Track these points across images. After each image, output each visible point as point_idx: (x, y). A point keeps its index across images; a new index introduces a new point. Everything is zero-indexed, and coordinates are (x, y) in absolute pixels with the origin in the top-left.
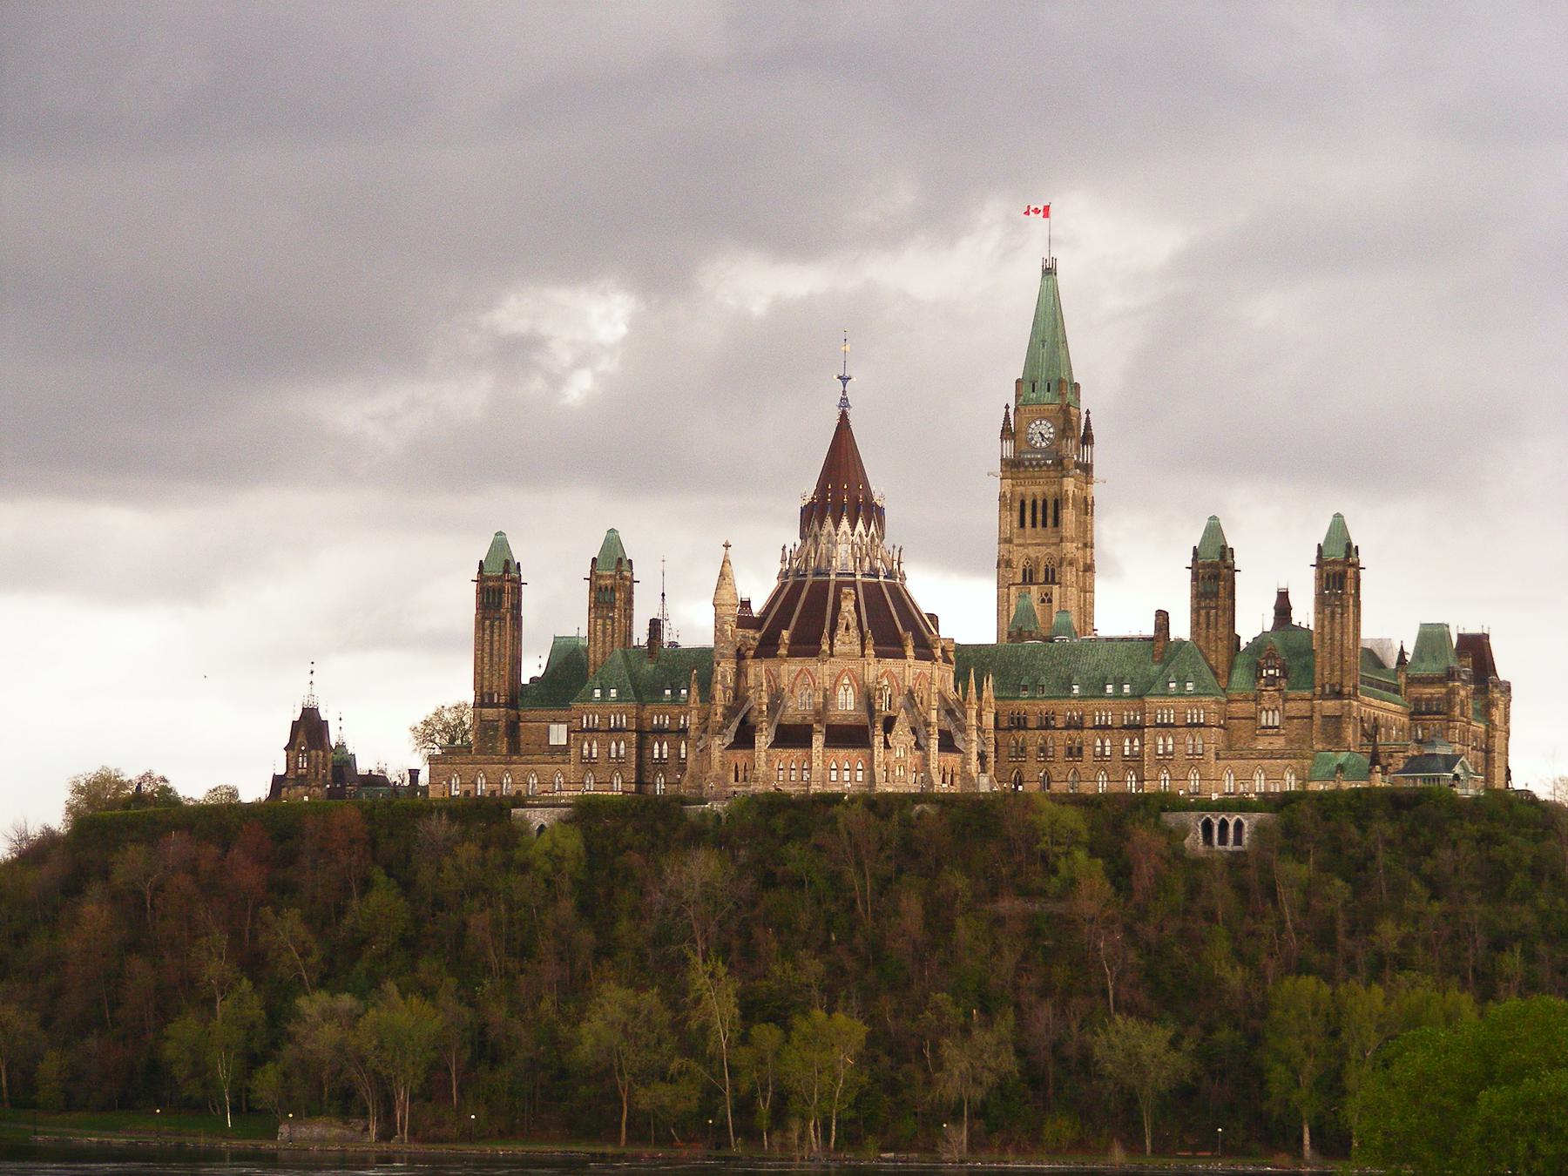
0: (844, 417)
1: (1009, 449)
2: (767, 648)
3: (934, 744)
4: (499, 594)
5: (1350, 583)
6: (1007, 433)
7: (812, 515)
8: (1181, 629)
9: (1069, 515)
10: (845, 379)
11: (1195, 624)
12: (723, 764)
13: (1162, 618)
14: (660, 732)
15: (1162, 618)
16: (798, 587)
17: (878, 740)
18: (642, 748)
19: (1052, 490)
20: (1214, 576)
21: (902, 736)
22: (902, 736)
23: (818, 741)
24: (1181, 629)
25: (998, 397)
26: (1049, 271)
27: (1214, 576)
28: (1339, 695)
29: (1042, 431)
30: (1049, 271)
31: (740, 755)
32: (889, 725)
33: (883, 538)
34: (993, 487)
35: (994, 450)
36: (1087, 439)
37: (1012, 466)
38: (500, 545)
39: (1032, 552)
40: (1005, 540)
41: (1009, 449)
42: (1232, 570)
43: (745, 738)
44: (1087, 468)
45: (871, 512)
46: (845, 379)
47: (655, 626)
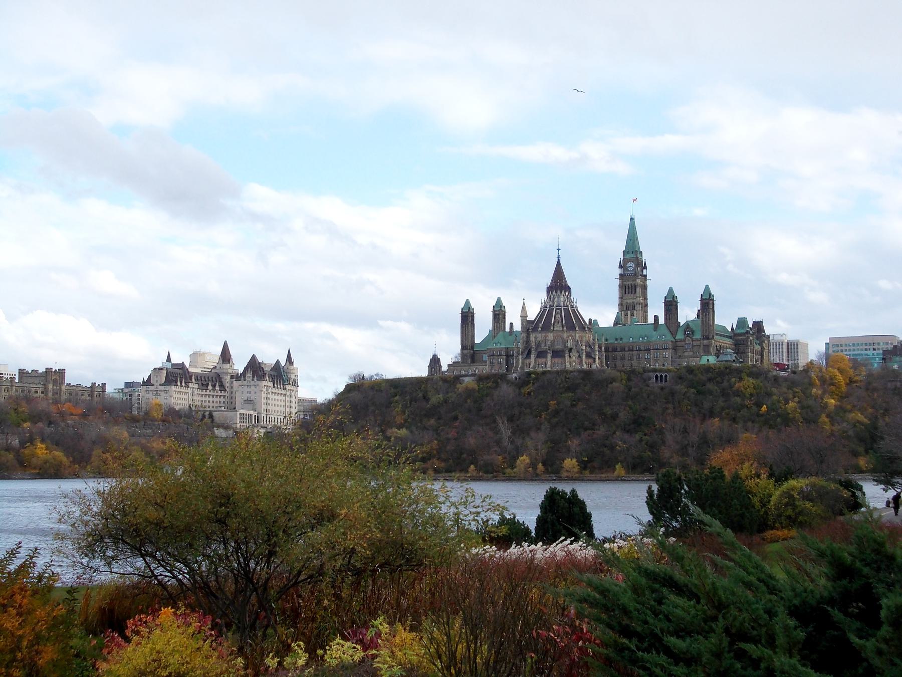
1: (621, 271)
2: (535, 329)
3: (584, 356)
4: (467, 317)
5: (711, 307)
6: (620, 267)
7: (550, 289)
8: (662, 321)
9: (639, 290)
11: (666, 319)
12: (523, 363)
16: (545, 310)
17: (567, 355)
18: (507, 360)
20: (671, 305)
21: (574, 355)
22: (574, 355)
23: (549, 356)
25: (618, 255)
26: (632, 219)
27: (671, 305)
28: (708, 339)
29: (631, 266)
30: (632, 219)
31: (527, 361)
32: (570, 350)
34: (618, 282)
35: (618, 272)
36: (645, 267)
37: (622, 276)
38: (467, 302)
39: (628, 301)
40: (621, 298)
41: (621, 271)
42: (677, 302)
43: (529, 355)
44: (645, 276)
45: (568, 289)
47: (511, 324)
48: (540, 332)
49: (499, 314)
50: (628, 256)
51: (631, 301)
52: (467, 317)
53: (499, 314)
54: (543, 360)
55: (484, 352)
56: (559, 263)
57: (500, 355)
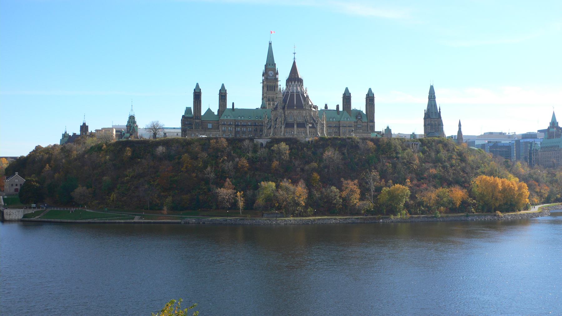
0: (294, 63)
8: (341, 109)
10: (294, 54)
13: (338, 106)
14: (238, 126)
15: (338, 106)
18: (235, 128)
19: (273, 84)
20: (347, 98)
24: (341, 109)
26: (270, 44)
27: (347, 98)
30: (270, 44)
33: (302, 85)
39: (270, 96)
46: (294, 54)
48: (295, 110)
49: (223, 95)
50: (270, 67)
51: (272, 96)
52: (197, 95)
53: (223, 95)
54: (302, 129)
55: (209, 122)
56: (294, 63)
57: (230, 125)
